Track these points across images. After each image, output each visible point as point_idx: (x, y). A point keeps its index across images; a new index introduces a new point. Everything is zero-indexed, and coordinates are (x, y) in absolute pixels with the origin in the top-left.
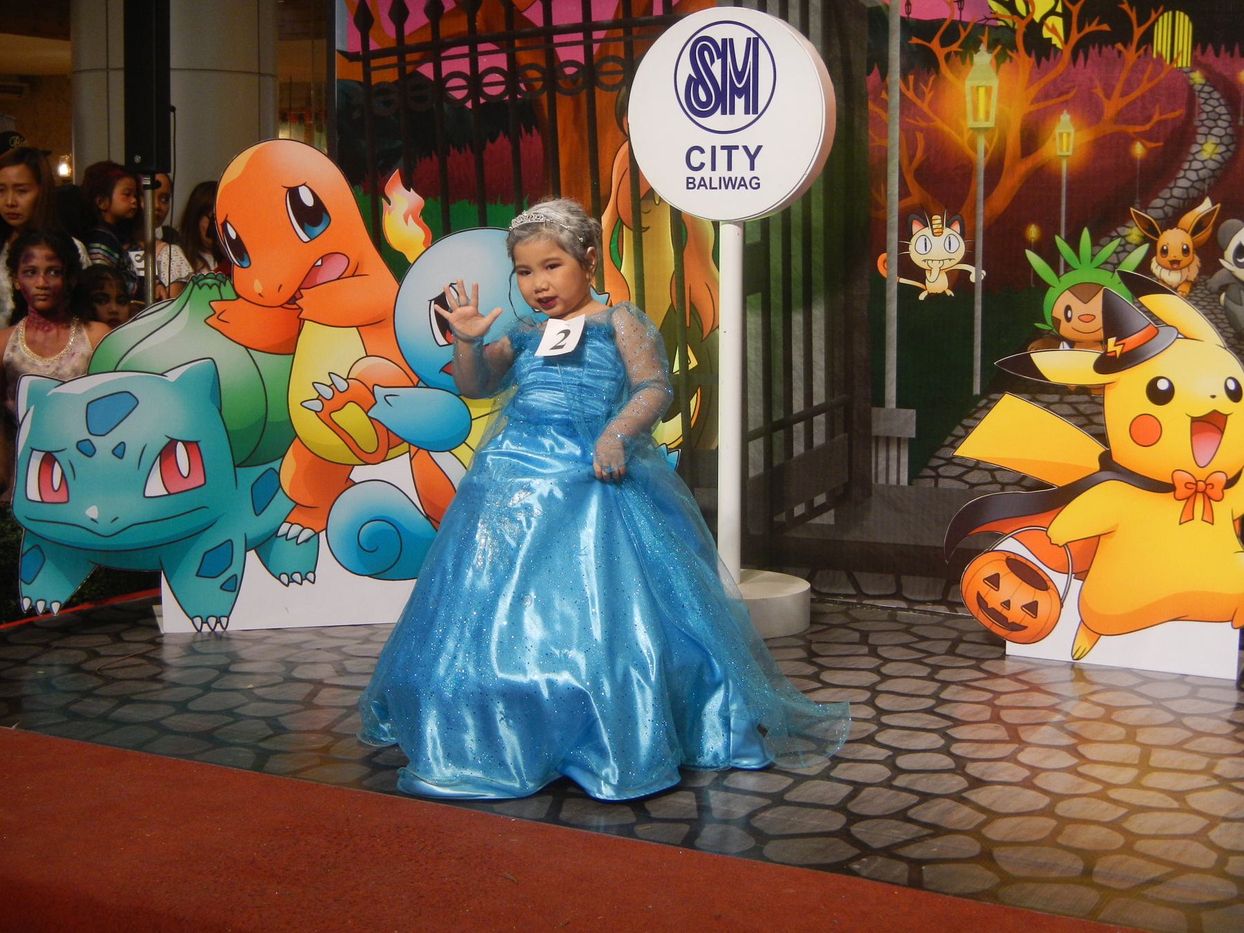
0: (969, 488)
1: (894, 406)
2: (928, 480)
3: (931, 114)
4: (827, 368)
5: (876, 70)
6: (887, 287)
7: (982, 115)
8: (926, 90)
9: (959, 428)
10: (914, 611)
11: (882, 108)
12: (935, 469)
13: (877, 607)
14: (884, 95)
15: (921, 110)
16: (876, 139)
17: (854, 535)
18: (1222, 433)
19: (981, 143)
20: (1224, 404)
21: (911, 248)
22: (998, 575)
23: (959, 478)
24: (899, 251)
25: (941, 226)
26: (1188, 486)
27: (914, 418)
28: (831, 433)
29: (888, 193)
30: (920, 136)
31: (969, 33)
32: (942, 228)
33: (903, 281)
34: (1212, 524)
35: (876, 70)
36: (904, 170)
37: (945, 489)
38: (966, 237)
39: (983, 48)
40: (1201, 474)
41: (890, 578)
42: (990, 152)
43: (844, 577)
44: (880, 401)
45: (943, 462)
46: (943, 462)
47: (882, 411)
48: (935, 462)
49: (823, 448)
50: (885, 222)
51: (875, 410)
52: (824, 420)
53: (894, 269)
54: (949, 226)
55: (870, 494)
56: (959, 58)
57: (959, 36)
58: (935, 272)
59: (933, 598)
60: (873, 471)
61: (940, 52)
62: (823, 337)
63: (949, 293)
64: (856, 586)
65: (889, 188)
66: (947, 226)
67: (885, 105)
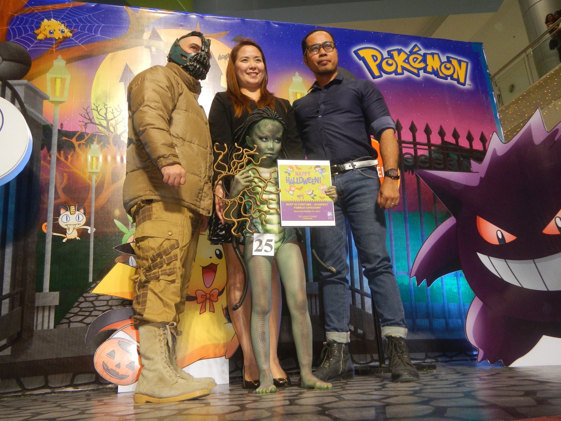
0: (87, 326)
1: (48, 291)
2: (65, 325)
3: (71, 166)
4: (11, 276)
5: (45, 148)
6: (47, 237)
7: (94, 167)
8: (69, 157)
9: (81, 298)
10: (55, 393)
11: (47, 163)
12: (68, 319)
13: (33, 395)
14: (48, 158)
15: (66, 164)
16: (44, 175)
17: (23, 358)
18: (216, 272)
19: (94, 178)
20: (215, 260)
21: (60, 220)
22: (114, 351)
23: (81, 321)
24: (53, 221)
25: (74, 211)
26: (203, 297)
27: (58, 296)
28: (12, 307)
29: (49, 197)
30: (65, 175)
31: (89, 137)
32: (75, 211)
33: (55, 234)
34: (214, 312)
35: (45, 148)
36: (57, 187)
37: (74, 328)
38: (87, 214)
39: (95, 143)
40: (208, 291)
41: (42, 378)
42: (98, 181)
43: (14, 381)
44: (40, 289)
45: (72, 315)
46: (72, 315)
47: (41, 294)
48: (68, 316)
49: (7, 315)
50: (47, 211)
51: (37, 294)
52: (8, 302)
53: (51, 229)
54: (78, 210)
55: (32, 336)
56: (84, 146)
57: (84, 138)
58: (71, 230)
59: (65, 384)
60: (35, 324)
61: (76, 144)
62: (11, 261)
63: (78, 238)
64: (21, 385)
65: (49, 195)
66: (77, 211)
67: (49, 162)
